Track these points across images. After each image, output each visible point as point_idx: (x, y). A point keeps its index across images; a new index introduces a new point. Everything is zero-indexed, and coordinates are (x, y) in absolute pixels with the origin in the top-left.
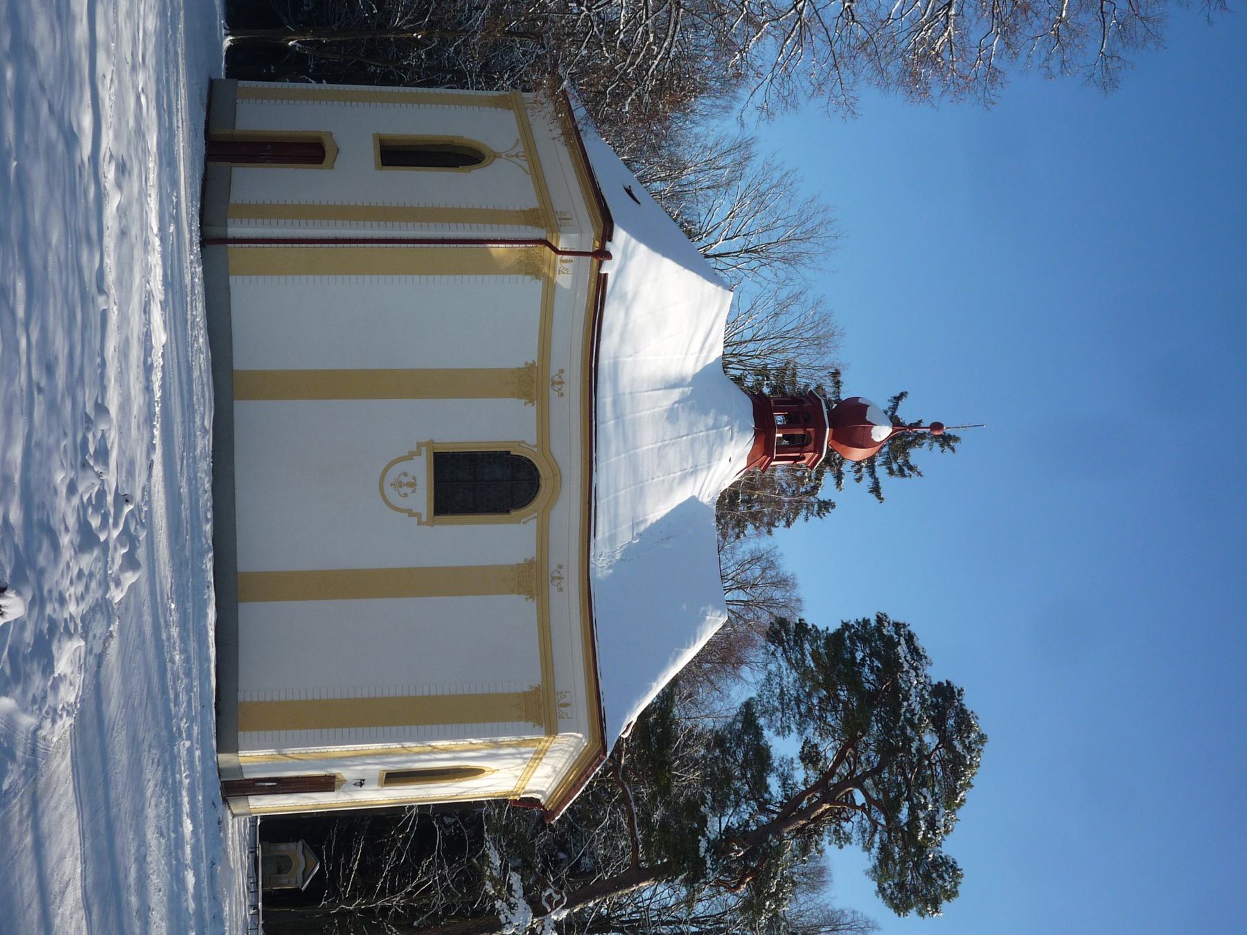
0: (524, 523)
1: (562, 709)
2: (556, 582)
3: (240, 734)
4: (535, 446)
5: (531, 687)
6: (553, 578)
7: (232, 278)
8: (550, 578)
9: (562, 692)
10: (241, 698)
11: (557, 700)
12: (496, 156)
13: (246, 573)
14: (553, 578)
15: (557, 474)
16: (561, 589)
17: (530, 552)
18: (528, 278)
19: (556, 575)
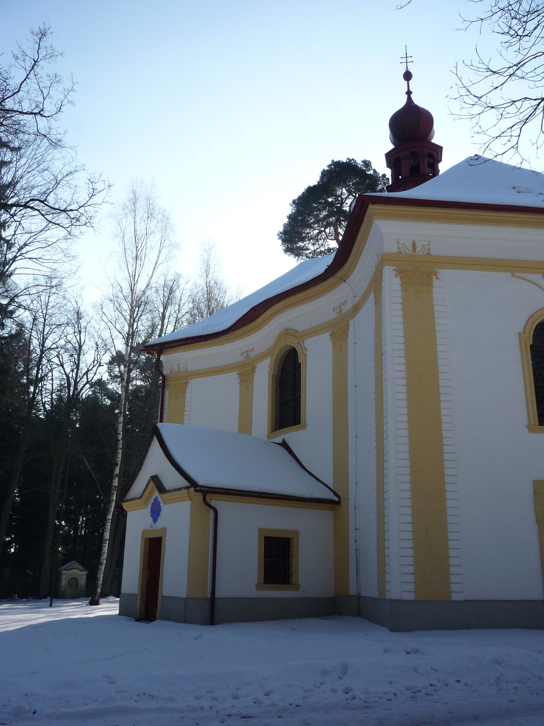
0: (306, 349)
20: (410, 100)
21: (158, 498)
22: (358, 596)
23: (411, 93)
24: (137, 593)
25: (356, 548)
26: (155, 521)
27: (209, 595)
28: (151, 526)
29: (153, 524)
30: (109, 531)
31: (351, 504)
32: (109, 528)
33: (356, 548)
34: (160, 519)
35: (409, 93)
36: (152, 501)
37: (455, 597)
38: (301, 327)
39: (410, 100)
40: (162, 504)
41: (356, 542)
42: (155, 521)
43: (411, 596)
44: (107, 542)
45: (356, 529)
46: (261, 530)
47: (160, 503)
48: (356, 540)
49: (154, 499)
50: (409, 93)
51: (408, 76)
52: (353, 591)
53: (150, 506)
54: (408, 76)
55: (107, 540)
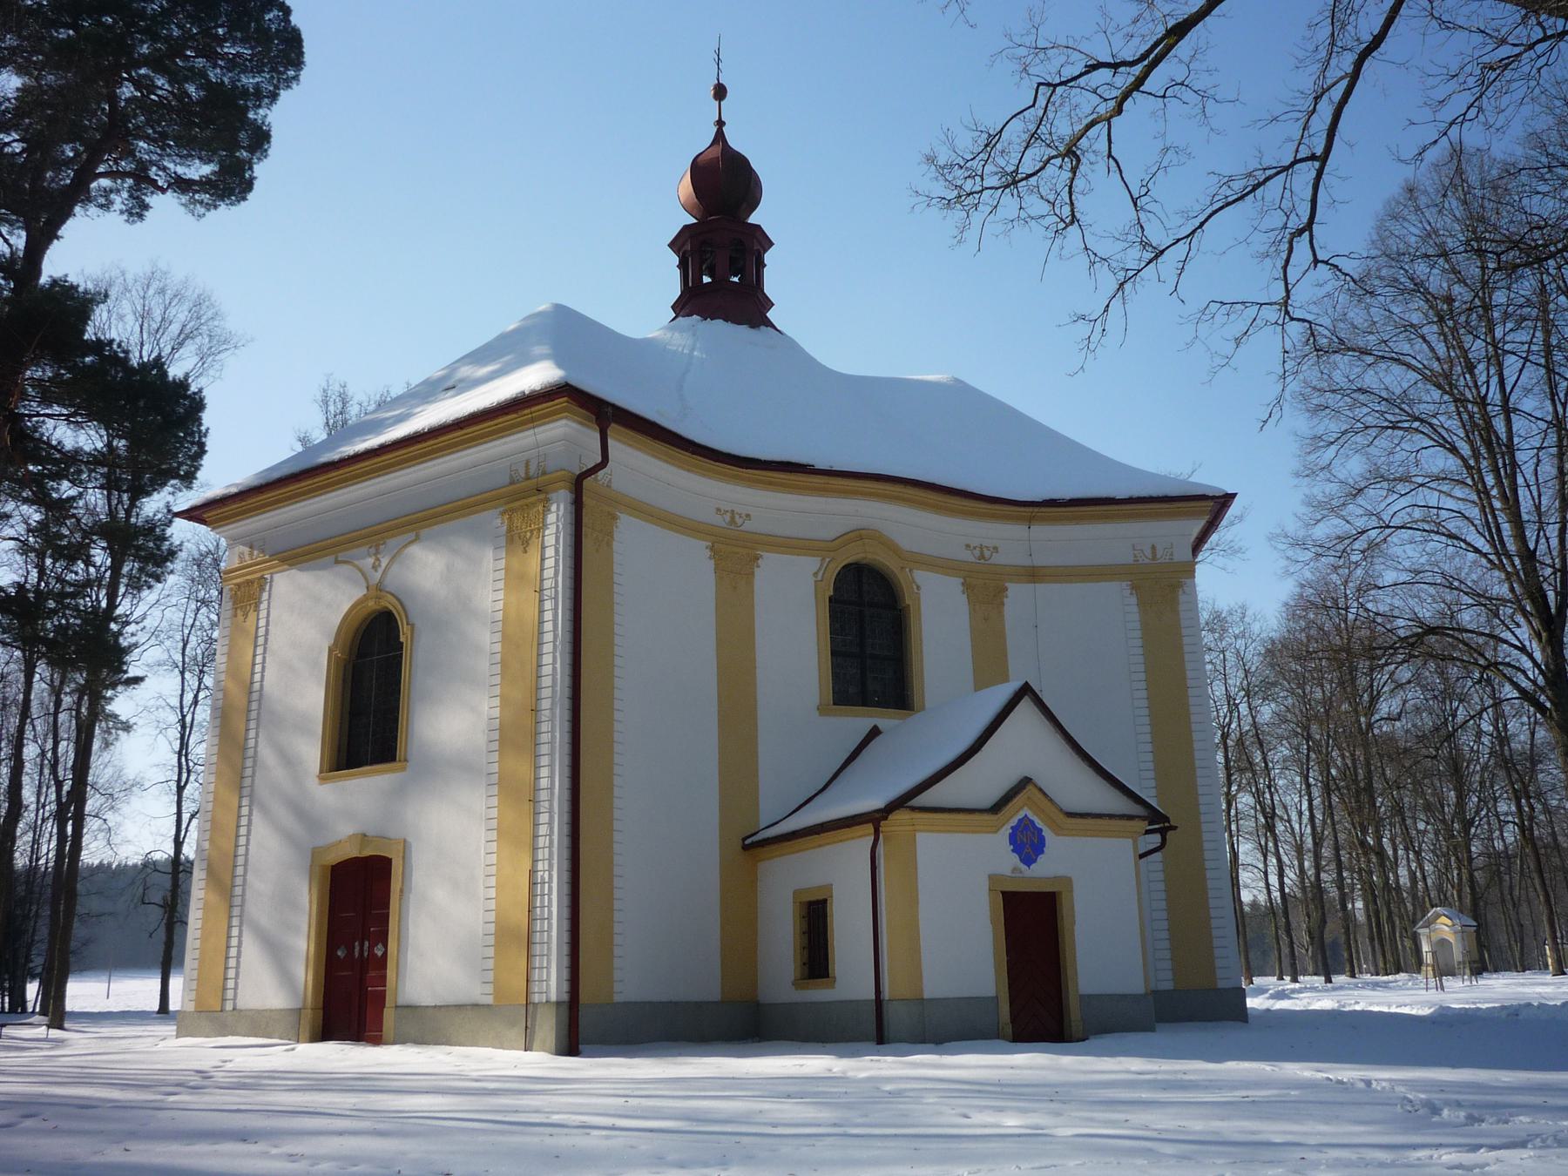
0: (918, 588)
1: (1158, 556)
2: (987, 553)
3: (1221, 984)
4: (823, 559)
5: (1131, 594)
6: (982, 556)
7: (618, 998)
8: (982, 561)
9: (1135, 556)
10: (1168, 986)
11: (1147, 561)
12: (378, 589)
13: (796, 1003)
14: (982, 556)
15: (859, 535)
16: (996, 549)
17: (954, 585)
19: (977, 552)
20: (720, 137)
21: (1032, 822)
23: (724, 123)
26: (1028, 861)
28: (1015, 870)
29: (1023, 867)
34: (1042, 859)
35: (720, 123)
36: (1014, 822)
38: (905, 543)
39: (720, 137)
40: (1047, 833)
42: (1028, 861)
47: (1041, 830)
49: (1020, 821)
50: (720, 123)
51: (720, 92)
53: (1006, 831)
54: (720, 92)
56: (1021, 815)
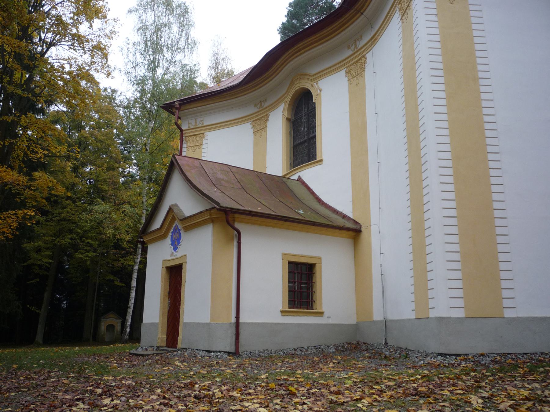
18: (204, 142)
21: (178, 226)
22: (386, 321)
24: (158, 322)
25: (381, 273)
26: (175, 249)
27: (233, 320)
28: (172, 255)
29: (174, 252)
30: (136, 279)
31: (374, 229)
32: (136, 277)
33: (381, 273)
36: (172, 230)
37: (508, 314)
41: (381, 266)
42: (175, 249)
43: (460, 314)
44: (135, 289)
45: (381, 254)
46: (284, 255)
48: (381, 265)
49: (175, 227)
52: (377, 316)
55: (135, 287)
56: (174, 225)
